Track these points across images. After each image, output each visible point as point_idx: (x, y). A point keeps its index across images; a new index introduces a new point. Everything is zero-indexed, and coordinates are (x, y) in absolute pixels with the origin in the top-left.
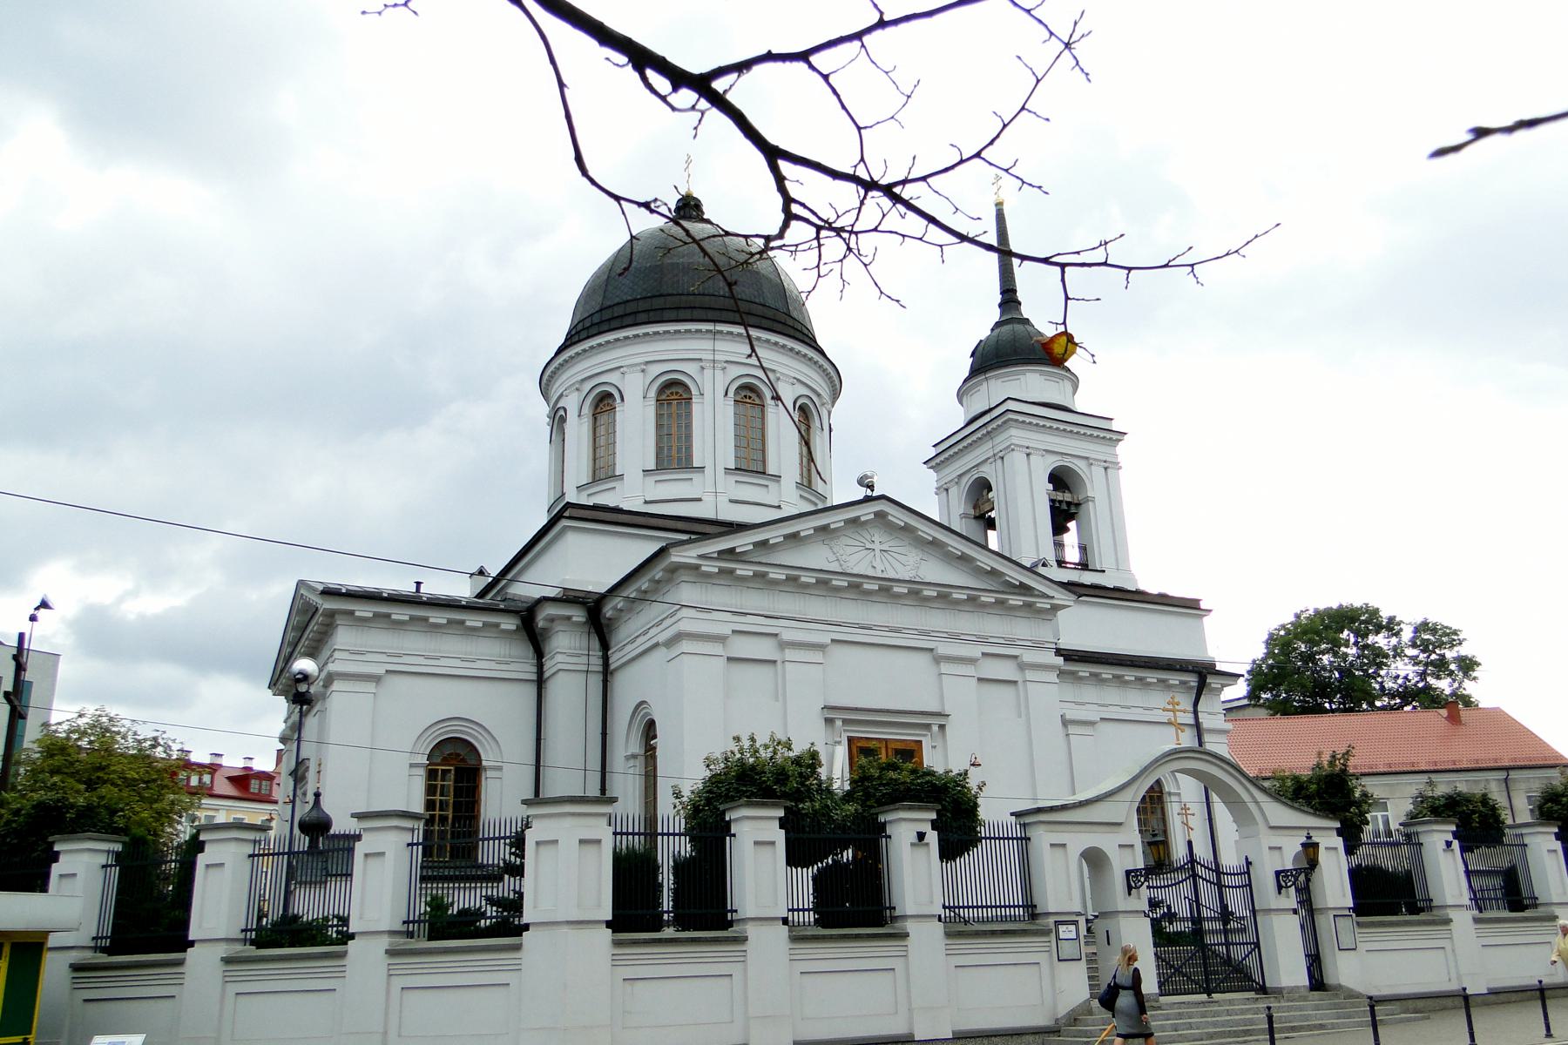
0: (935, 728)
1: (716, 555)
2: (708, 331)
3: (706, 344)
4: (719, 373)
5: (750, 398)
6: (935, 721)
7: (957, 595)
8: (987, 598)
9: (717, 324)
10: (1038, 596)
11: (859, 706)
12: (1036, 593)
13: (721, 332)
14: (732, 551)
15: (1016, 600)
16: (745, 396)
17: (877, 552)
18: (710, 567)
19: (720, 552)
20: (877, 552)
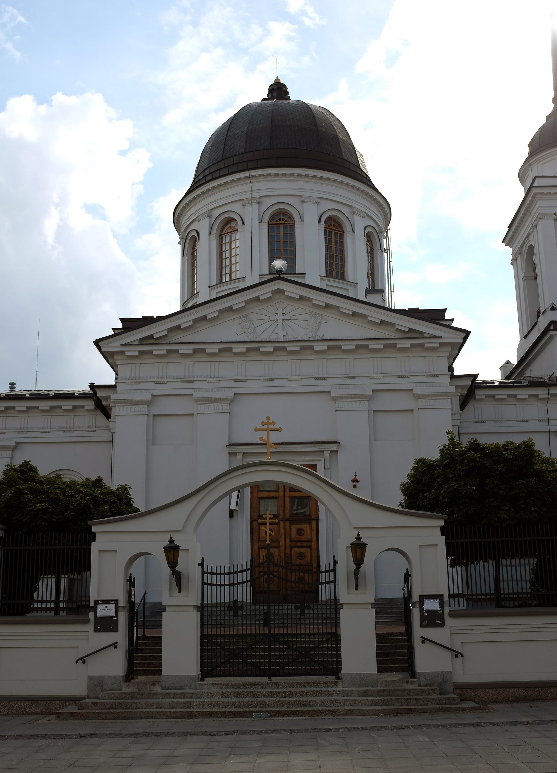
0: (327, 455)
1: (137, 342)
2: (245, 178)
3: (246, 187)
4: (255, 207)
5: (283, 220)
6: (327, 448)
7: (346, 346)
8: (378, 345)
9: (250, 171)
10: (426, 337)
11: (254, 442)
12: (426, 335)
13: (255, 176)
14: (151, 337)
15: (402, 344)
16: (280, 220)
17: (280, 322)
18: (133, 351)
19: (141, 340)
20: (280, 322)
